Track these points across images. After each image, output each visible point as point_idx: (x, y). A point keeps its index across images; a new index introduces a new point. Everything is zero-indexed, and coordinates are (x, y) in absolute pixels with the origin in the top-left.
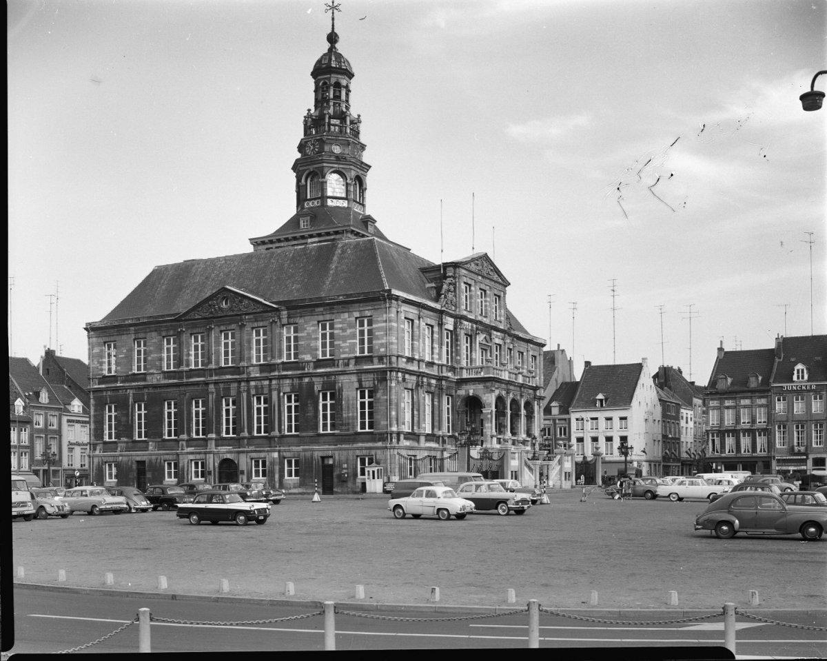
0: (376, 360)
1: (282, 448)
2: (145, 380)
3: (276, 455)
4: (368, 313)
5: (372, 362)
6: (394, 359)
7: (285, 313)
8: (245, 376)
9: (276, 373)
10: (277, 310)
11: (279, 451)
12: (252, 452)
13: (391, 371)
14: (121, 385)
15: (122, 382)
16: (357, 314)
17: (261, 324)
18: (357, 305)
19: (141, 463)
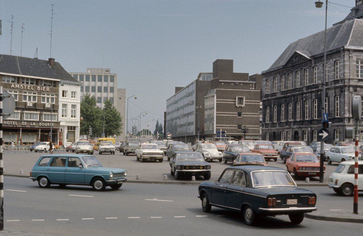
0: (340, 82)
1: (312, 126)
2: (276, 96)
3: (309, 129)
4: (338, 58)
5: (339, 82)
6: (346, 81)
7: (313, 61)
8: (301, 92)
9: (310, 90)
10: (310, 60)
11: (311, 127)
12: (304, 127)
13: (345, 87)
14: (265, 99)
15: (271, 97)
16: (334, 60)
17: (306, 67)
18: (334, 55)
19: (274, 133)
